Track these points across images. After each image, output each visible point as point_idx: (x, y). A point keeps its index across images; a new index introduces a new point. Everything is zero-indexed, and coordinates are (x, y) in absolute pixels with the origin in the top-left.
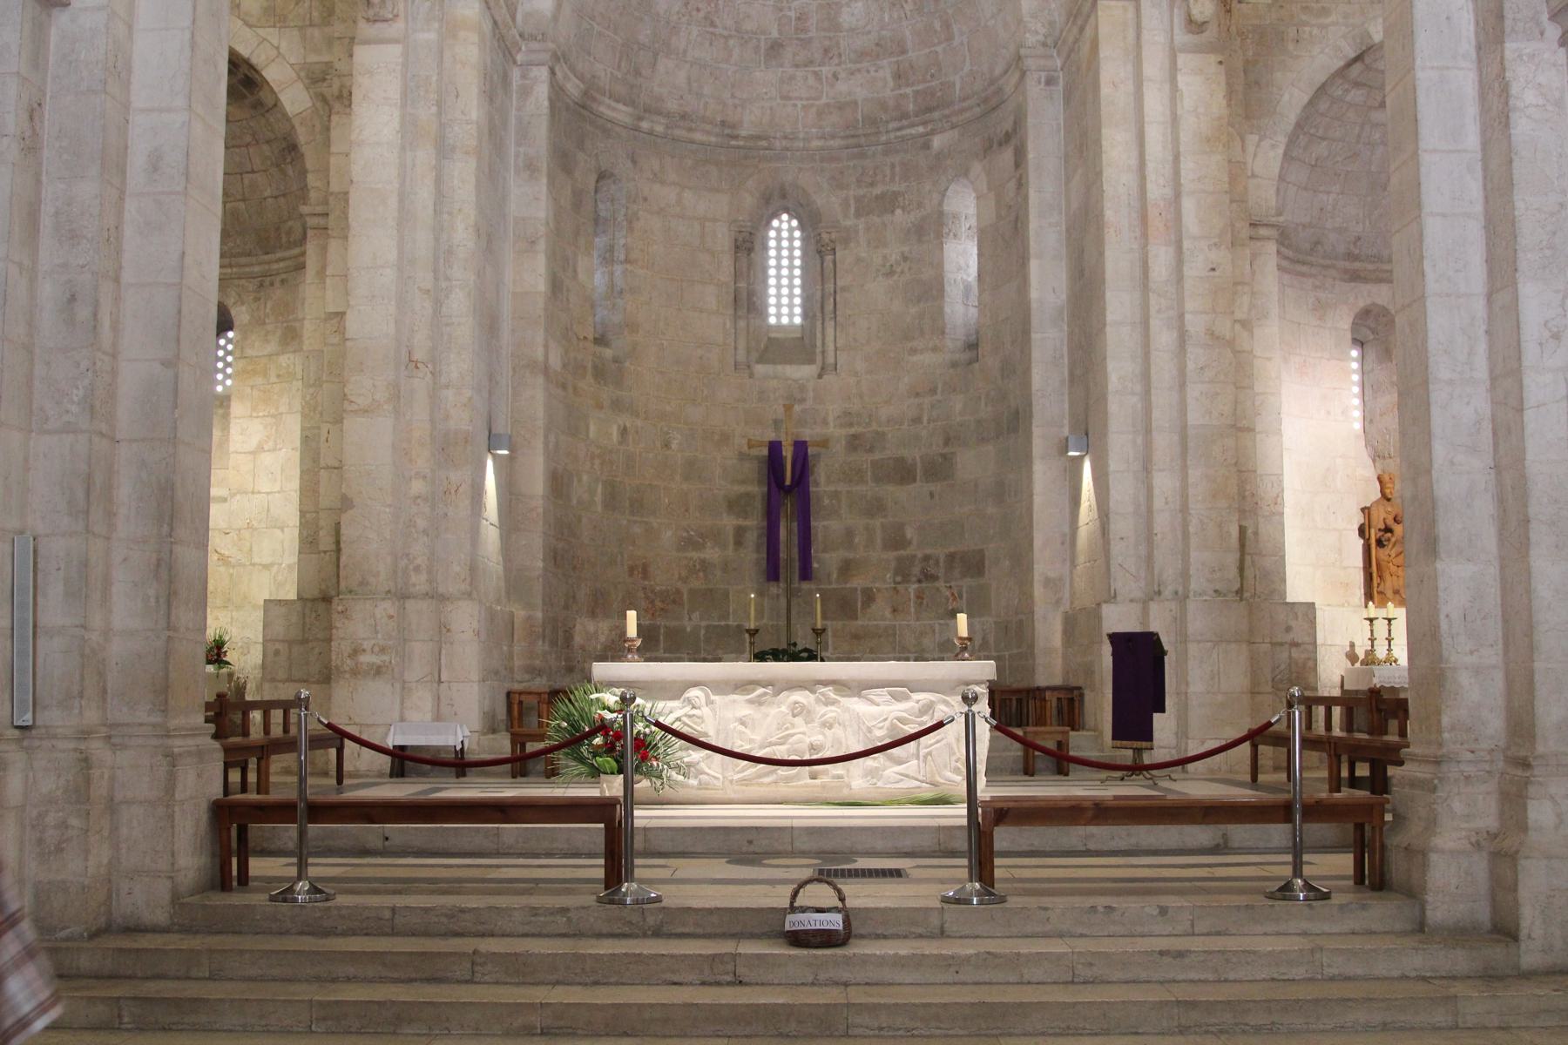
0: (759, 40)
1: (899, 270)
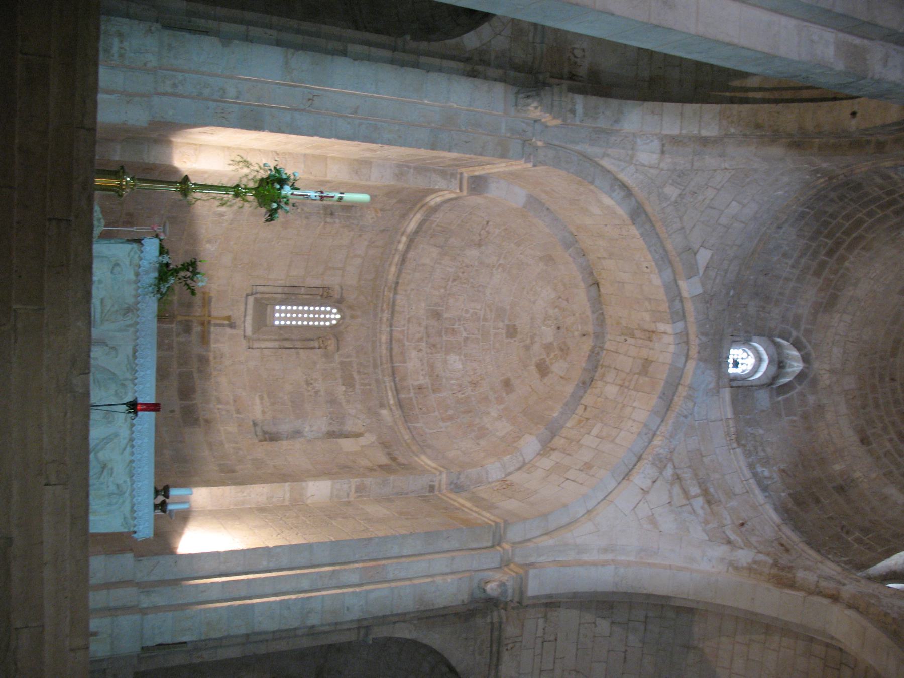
0: (443, 306)
1: (310, 389)
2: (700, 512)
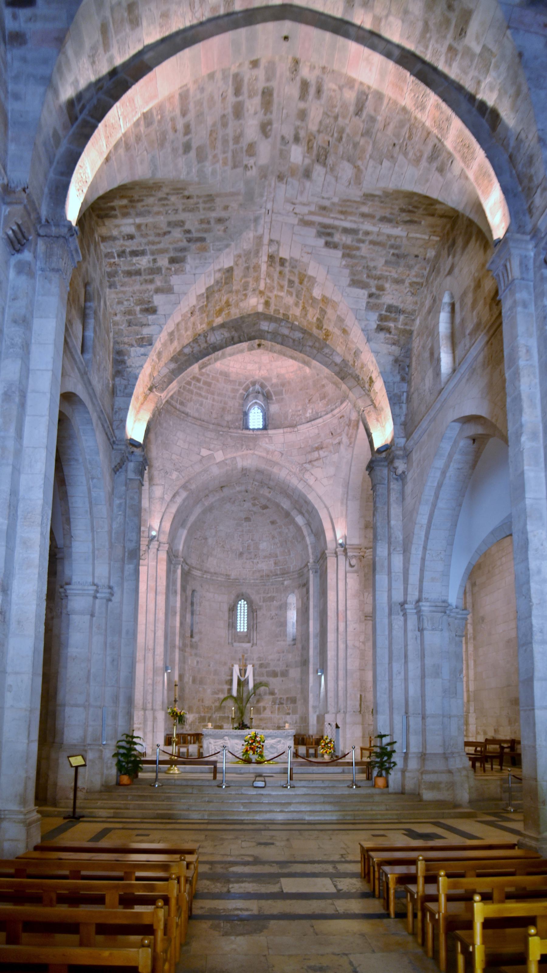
2: (326, 454)
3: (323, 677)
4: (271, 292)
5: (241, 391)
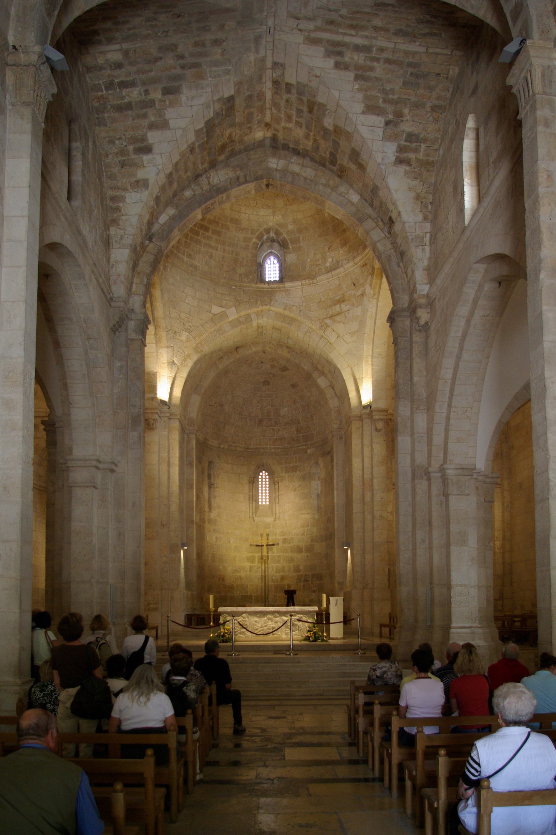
2: (348, 307)
3: (349, 551)
4: (279, 123)
5: (254, 240)
